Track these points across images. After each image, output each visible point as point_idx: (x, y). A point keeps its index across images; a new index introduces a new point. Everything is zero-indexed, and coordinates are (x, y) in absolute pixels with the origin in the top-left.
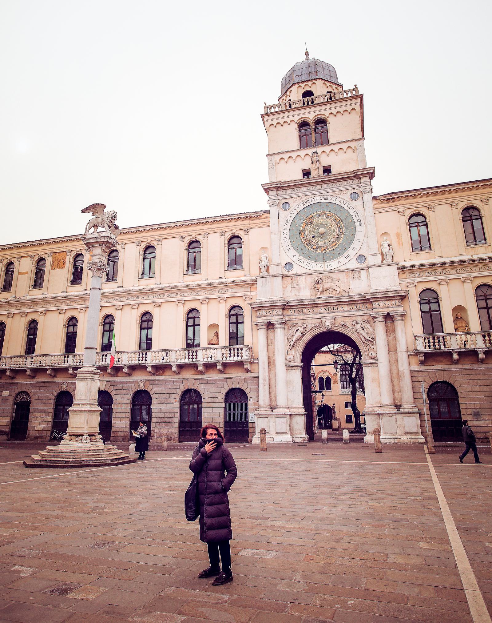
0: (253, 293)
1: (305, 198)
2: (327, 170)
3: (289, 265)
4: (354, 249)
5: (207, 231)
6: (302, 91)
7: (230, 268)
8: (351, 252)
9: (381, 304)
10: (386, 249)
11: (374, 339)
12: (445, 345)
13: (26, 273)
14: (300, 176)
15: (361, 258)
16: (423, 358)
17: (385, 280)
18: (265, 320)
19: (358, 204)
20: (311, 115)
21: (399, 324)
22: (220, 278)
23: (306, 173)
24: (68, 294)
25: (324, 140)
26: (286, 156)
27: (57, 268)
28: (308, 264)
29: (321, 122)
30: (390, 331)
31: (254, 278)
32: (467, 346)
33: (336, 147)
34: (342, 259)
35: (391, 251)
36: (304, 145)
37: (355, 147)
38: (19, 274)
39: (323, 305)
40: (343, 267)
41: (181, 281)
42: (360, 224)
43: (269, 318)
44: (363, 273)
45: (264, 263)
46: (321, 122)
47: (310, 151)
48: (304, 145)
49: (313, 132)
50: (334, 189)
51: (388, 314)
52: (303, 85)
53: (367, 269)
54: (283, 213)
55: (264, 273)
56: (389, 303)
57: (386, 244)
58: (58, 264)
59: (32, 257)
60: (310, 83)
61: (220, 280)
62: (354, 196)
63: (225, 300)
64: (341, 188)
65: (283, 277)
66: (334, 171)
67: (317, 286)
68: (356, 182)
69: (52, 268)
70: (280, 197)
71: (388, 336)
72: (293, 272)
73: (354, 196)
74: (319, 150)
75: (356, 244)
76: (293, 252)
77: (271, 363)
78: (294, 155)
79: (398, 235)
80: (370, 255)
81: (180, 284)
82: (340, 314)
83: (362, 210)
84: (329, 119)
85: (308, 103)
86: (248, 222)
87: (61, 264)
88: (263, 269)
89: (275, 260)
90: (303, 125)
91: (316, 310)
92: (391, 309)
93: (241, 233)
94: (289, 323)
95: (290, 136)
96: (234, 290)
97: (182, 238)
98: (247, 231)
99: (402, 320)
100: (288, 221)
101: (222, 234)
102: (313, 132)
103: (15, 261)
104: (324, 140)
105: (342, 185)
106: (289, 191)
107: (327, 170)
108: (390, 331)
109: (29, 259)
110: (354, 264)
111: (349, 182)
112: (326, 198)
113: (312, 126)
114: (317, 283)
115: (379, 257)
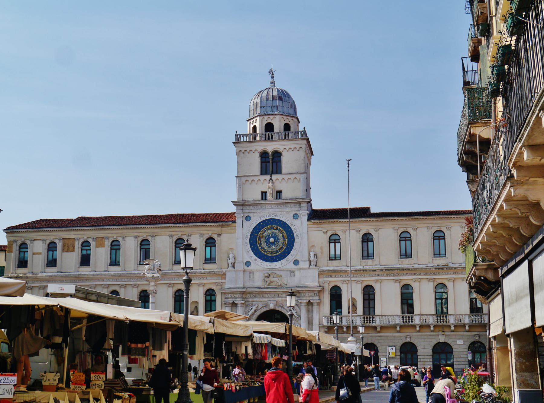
0: (223, 281)
1: (261, 214)
2: (279, 193)
3: (248, 264)
4: (292, 255)
5: (190, 233)
6: (265, 123)
7: (207, 262)
8: (291, 257)
9: (306, 294)
10: (312, 258)
11: (300, 316)
12: (412, 322)
13: (40, 253)
14: (259, 197)
15: (296, 262)
16: (326, 330)
17: (309, 278)
18: (230, 301)
19: (297, 222)
20: (270, 147)
21: (315, 307)
22: (200, 269)
23: (264, 194)
24: (80, 273)
25: (278, 170)
26: (250, 179)
27: (67, 251)
28: (261, 263)
29: (277, 155)
30: (309, 311)
31: (224, 271)
32: (391, 323)
33: (286, 177)
34: (283, 261)
35: (316, 259)
36: (264, 171)
37: (300, 179)
38: (33, 254)
39: (270, 293)
40: (284, 268)
41: (171, 270)
42: (298, 238)
43: (233, 299)
44: (297, 273)
45: (231, 261)
46: (277, 155)
47: (268, 177)
48: (264, 171)
49: (271, 163)
50: (282, 210)
51: (309, 301)
52: (266, 117)
53: (300, 269)
54: (246, 224)
55: (231, 268)
56: (311, 294)
57: (312, 254)
58: (68, 247)
59: (44, 240)
60: (271, 117)
61: (200, 271)
62: (295, 216)
63: (203, 285)
64: (287, 209)
65: (244, 271)
66: (283, 195)
67: (266, 279)
68: (298, 205)
69: (63, 251)
70: (244, 211)
71: (308, 315)
72: (251, 268)
73: (295, 216)
74: (274, 177)
75: (293, 252)
76: (252, 254)
78: (256, 179)
79: (322, 248)
80: (302, 261)
81: (170, 271)
82: (280, 299)
83: (301, 227)
84: (283, 153)
85: (269, 138)
86: (220, 228)
87: (71, 248)
88: (230, 265)
89: (239, 259)
90: (264, 155)
91: (266, 295)
92: (311, 298)
93: (215, 237)
94: (247, 303)
95: (254, 163)
96: (209, 278)
97: (171, 236)
98: (219, 235)
99: (318, 305)
100: (249, 230)
101: (202, 236)
102: (271, 163)
103: (28, 242)
104: (278, 170)
105: (288, 209)
106: (251, 207)
107: (279, 193)
108: (309, 311)
109: (41, 242)
111: (293, 205)
112: (277, 216)
113: (271, 157)
114: (267, 277)
115: (308, 262)
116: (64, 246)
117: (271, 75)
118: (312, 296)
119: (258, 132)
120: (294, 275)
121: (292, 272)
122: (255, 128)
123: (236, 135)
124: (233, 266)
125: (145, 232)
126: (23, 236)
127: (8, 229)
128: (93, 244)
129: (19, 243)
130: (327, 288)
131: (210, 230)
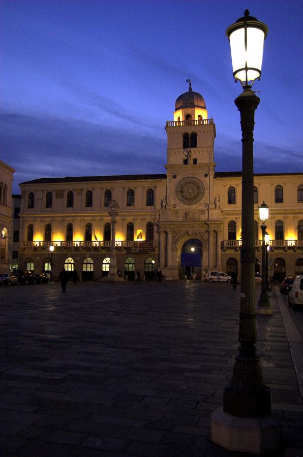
2: (195, 161)
14: (182, 163)
15: (207, 205)
17: (215, 214)
19: (207, 179)
23: (186, 162)
25: (194, 145)
34: (198, 204)
54: (173, 180)
58: (60, 195)
66: (198, 162)
69: (56, 198)
74: (192, 149)
76: (177, 200)
77: (166, 248)
104: (194, 145)
110: (203, 207)
116: (56, 194)
117: (189, 83)
118: (217, 227)
119: (181, 120)
120: (205, 214)
121: (202, 212)
122: (179, 118)
123: (167, 122)
124: (165, 207)
125: (108, 185)
126: (33, 188)
127: (21, 184)
128: (75, 193)
129: (28, 192)
130: (227, 221)
131: (148, 184)
